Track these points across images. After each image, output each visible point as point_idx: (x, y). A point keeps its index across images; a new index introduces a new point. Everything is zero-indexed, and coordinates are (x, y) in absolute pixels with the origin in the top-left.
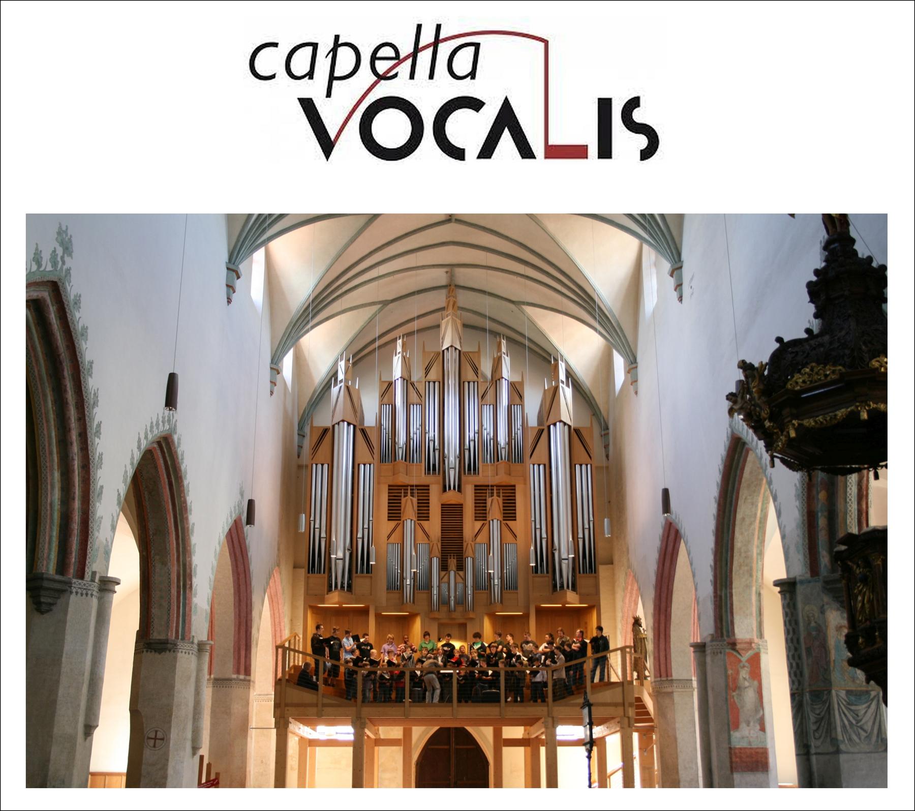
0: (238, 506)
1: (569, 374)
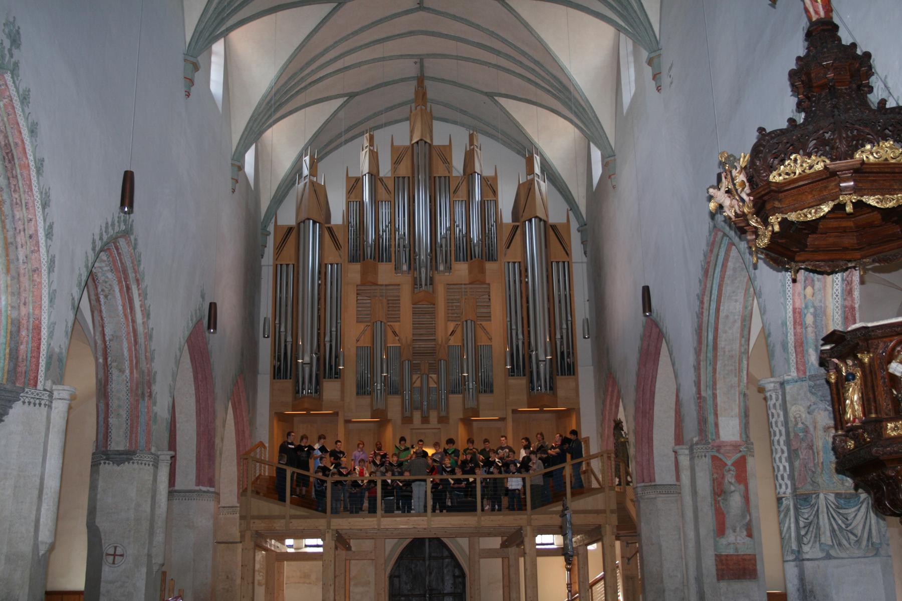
0: (200, 310)
1: (546, 167)
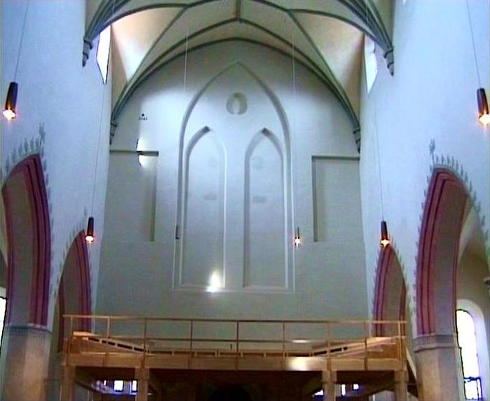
0: (37, 146)
